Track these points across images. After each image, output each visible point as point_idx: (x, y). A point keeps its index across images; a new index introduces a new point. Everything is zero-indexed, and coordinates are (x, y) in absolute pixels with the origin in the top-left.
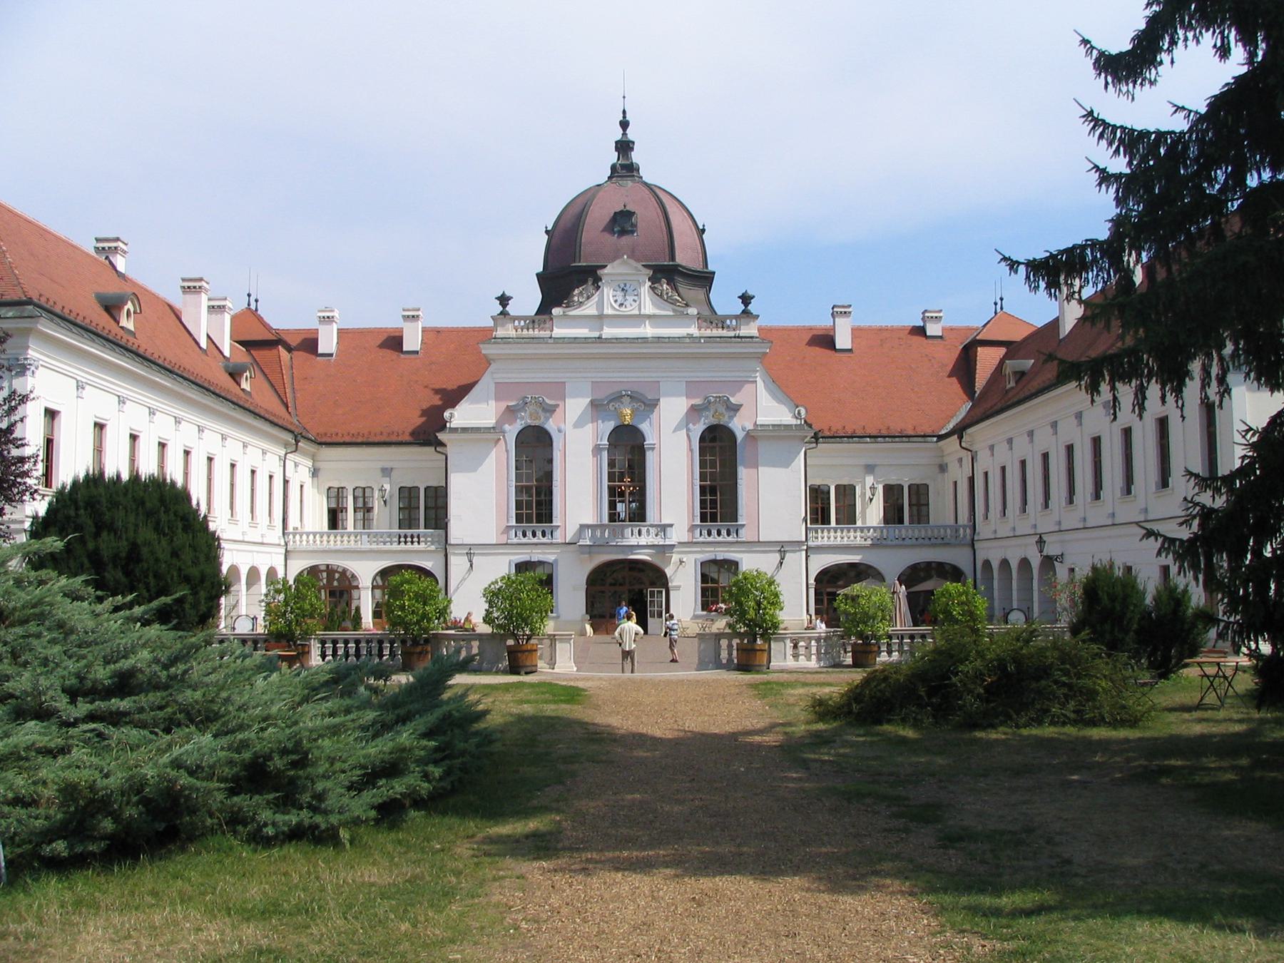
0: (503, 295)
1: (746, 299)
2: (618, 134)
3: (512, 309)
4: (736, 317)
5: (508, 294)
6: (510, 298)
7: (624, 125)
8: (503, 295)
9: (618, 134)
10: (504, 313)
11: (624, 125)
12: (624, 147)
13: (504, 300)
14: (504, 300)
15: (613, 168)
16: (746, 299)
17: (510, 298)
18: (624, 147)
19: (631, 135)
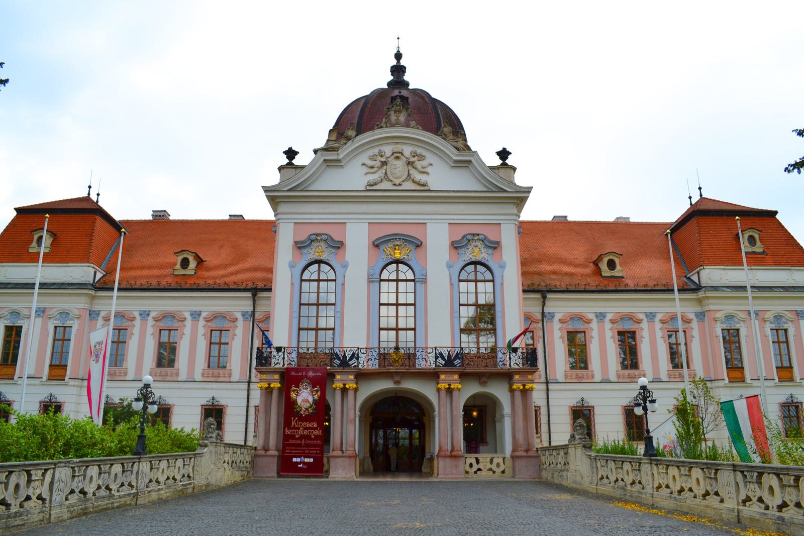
0: (290, 149)
1: (504, 154)
2: (394, 62)
3: (297, 161)
4: (497, 168)
5: (294, 149)
6: (296, 153)
7: (398, 56)
8: (290, 149)
9: (394, 62)
10: (290, 165)
11: (398, 56)
12: (398, 70)
13: (291, 154)
14: (291, 154)
15: (389, 84)
16: (504, 154)
17: (296, 153)
18: (398, 70)
19: (402, 62)
